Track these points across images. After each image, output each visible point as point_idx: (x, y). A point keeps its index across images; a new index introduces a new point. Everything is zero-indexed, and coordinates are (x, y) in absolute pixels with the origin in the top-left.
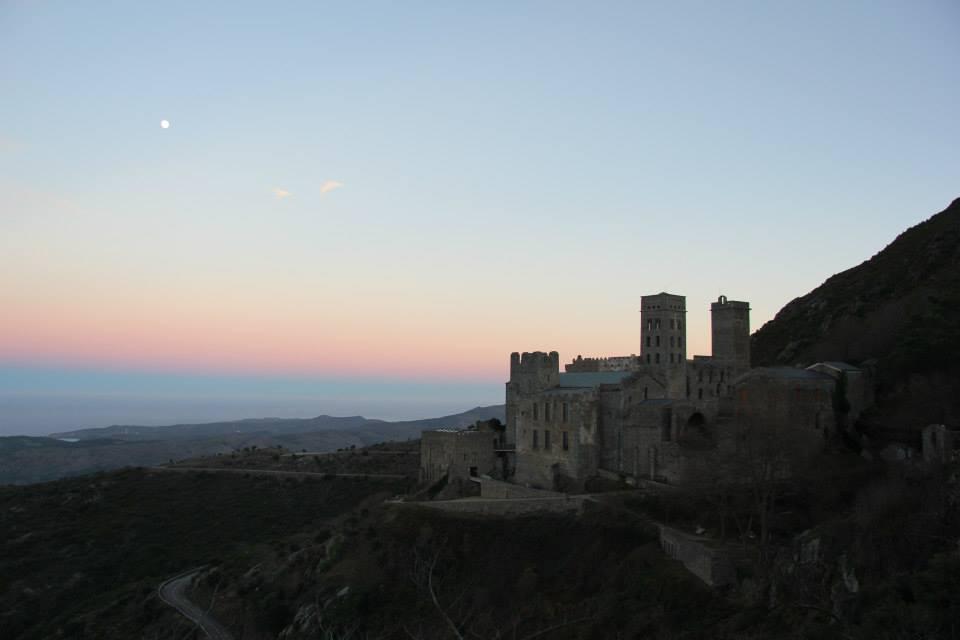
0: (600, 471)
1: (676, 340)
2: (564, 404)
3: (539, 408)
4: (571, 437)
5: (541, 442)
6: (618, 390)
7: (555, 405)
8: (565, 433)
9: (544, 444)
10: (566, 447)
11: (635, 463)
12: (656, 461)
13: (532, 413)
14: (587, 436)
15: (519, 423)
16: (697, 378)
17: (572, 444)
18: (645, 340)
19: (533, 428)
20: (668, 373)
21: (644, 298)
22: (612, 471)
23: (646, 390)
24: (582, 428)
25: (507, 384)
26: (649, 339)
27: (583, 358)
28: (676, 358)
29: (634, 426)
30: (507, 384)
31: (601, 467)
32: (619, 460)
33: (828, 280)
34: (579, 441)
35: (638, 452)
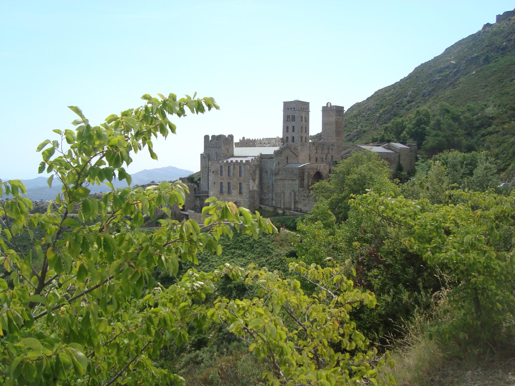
0: (262, 206)
1: (304, 128)
2: (240, 167)
3: (223, 169)
4: (244, 186)
5: (225, 189)
6: (271, 158)
7: (234, 167)
8: (240, 183)
9: (227, 190)
10: (240, 193)
11: (282, 201)
12: (295, 199)
13: (219, 172)
14: (254, 186)
15: (211, 178)
16: (315, 151)
17: (245, 190)
18: (286, 128)
19: (220, 181)
20: (299, 148)
21: (286, 104)
22: (268, 205)
23: (287, 157)
24: (251, 181)
25: (201, 155)
26: (288, 127)
27: (246, 138)
28: (304, 139)
29: (282, 179)
30: (201, 155)
31: (261, 203)
32: (272, 199)
33: (376, 93)
34: (249, 188)
35: (284, 194)
